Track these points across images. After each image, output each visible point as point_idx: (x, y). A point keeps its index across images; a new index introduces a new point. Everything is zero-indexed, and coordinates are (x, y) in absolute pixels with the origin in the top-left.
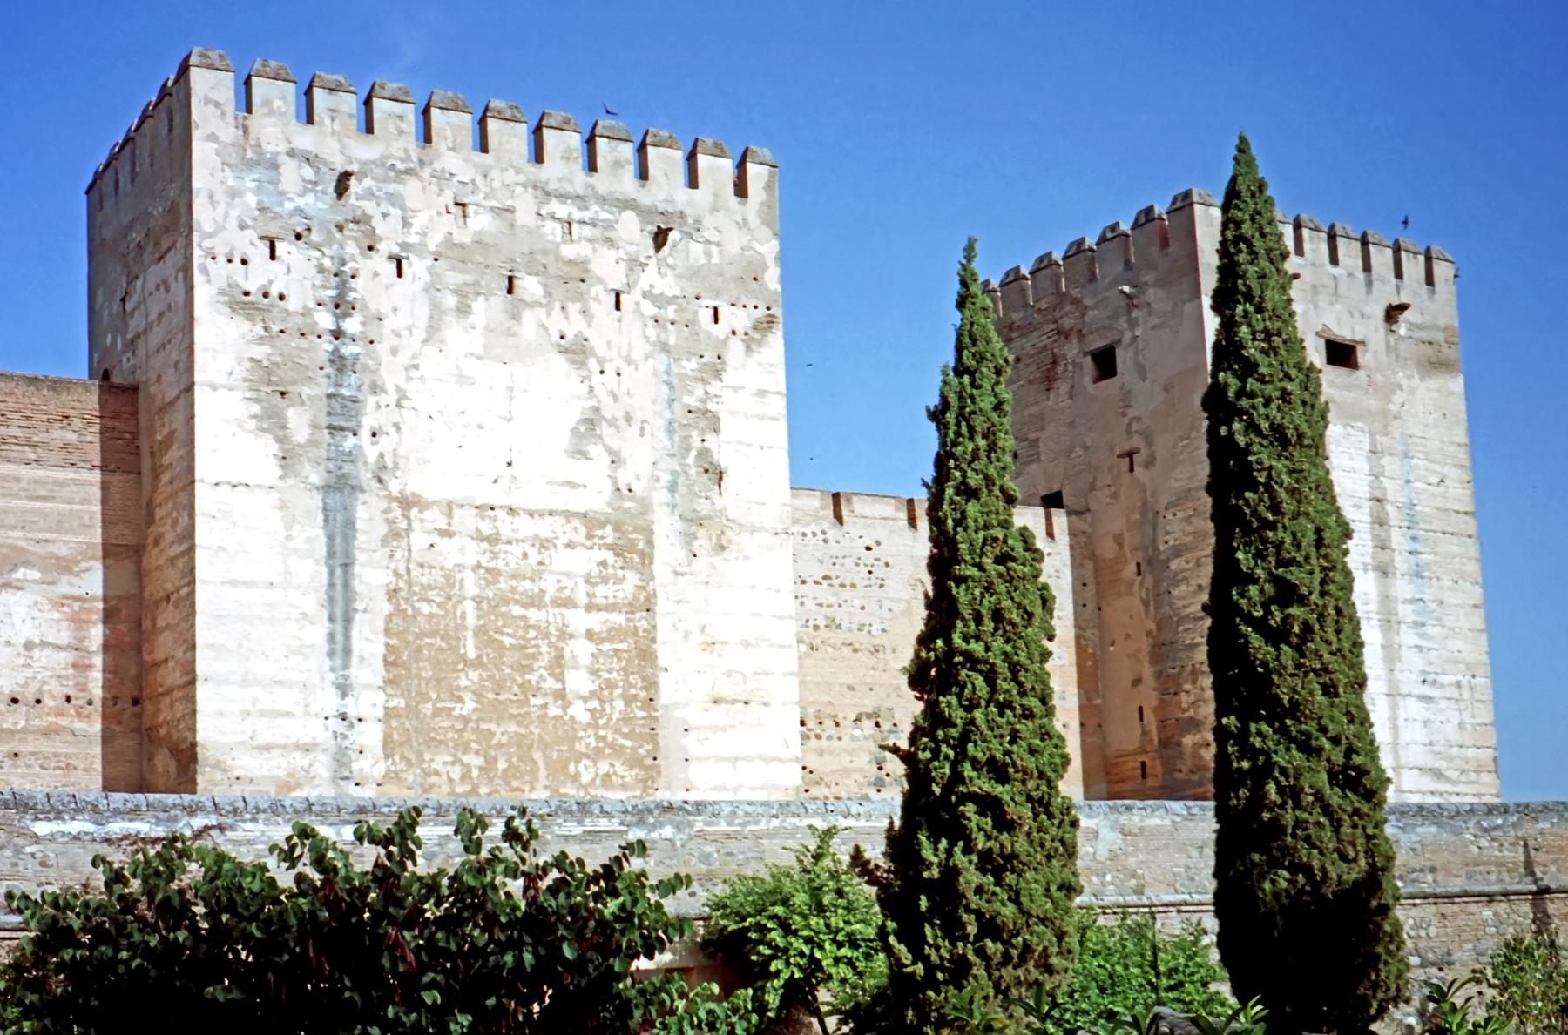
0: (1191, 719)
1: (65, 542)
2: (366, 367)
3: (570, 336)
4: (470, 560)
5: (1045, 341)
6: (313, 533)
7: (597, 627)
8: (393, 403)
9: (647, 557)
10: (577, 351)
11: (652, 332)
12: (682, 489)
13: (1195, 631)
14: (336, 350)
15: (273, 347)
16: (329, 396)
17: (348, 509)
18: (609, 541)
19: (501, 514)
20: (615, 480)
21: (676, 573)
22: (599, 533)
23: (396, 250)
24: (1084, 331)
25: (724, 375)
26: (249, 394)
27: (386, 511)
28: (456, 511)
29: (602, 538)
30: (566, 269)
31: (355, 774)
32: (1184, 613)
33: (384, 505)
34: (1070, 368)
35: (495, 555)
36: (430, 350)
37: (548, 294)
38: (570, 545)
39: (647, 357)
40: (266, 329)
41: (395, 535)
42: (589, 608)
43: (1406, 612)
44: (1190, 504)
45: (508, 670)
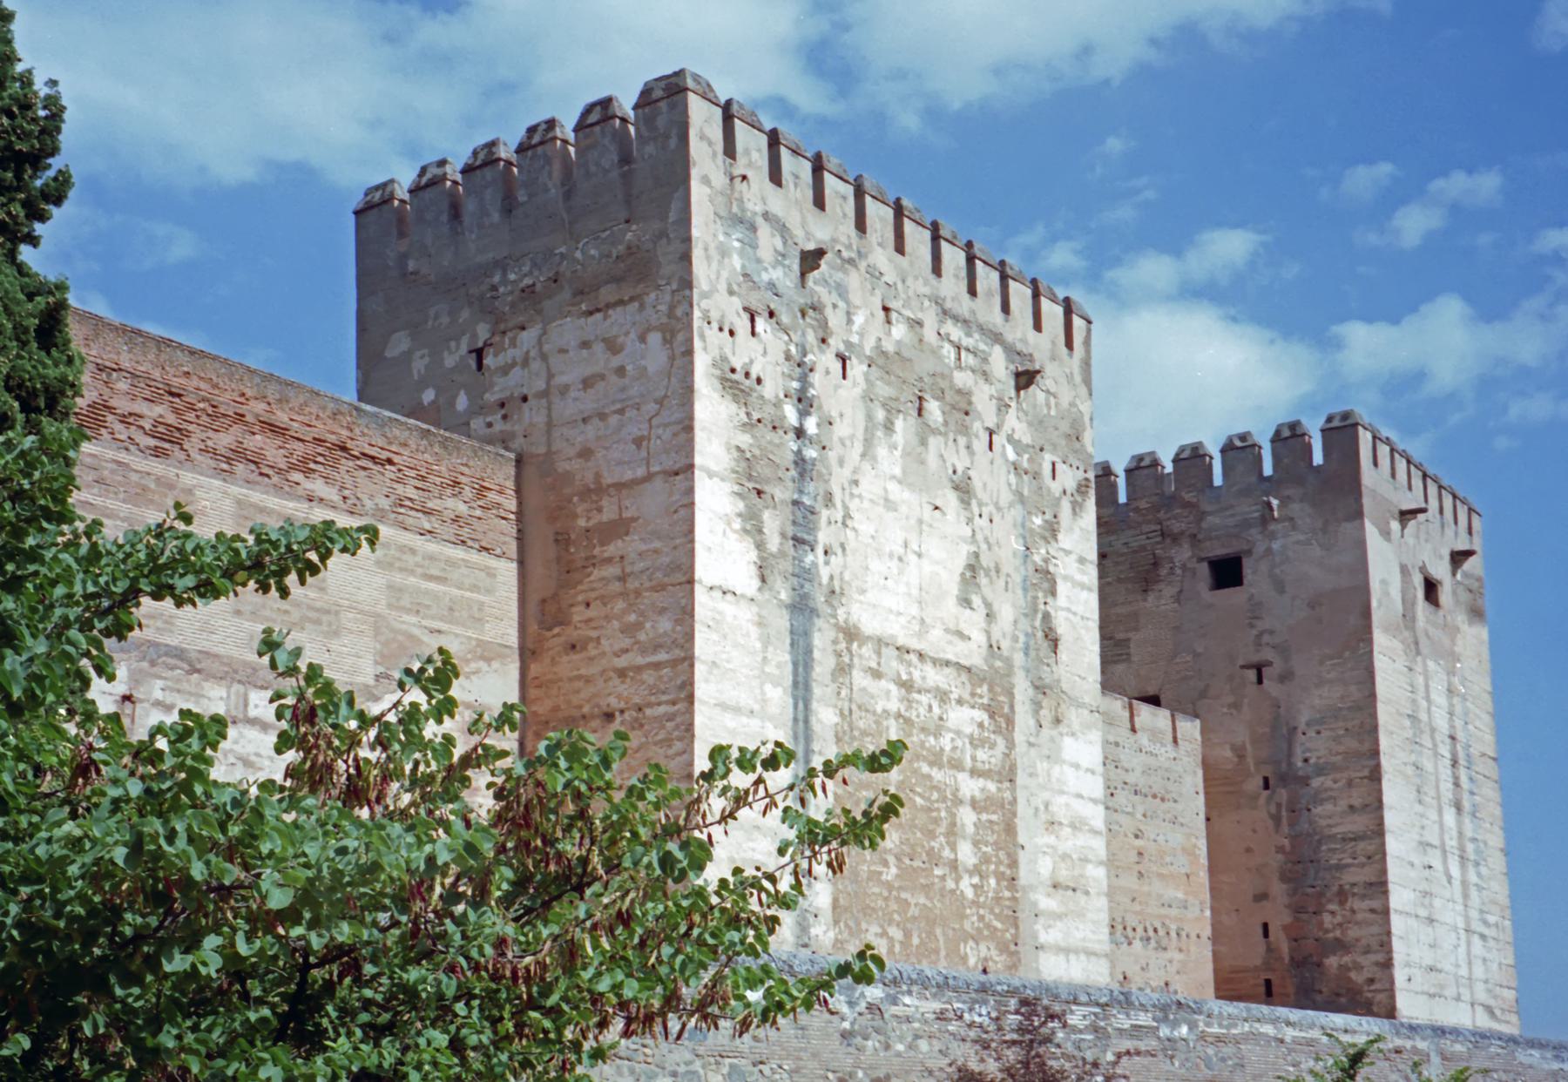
0: (1336, 939)
1: (457, 635)
2: (820, 475)
3: (960, 471)
4: (894, 705)
5: (1142, 541)
6: (781, 656)
7: (978, 794)
8: (840, 520)
9: (1010, 722)
10: (963, 489)
11: (1013, 479)
12: (1033, 653)
13: (1344, 852)
14: (799, 452)
15: (753, 436)
16: (796, 503)
17: (807, 634)
18: (985, 701)
19: (913, 658)
20: (989, 638)
21: (1031, 744)
22: (979, 691)
23: (842, 348)
24: (1200, 536)
25: (1060, 537)
26: (736, 488)
27: (835, 642)
28: (884, 650)
29: (981, 697)
30: (958, 398)
31: (812, 942)
32: (1327, 832)
33: (832, 634)
34: (1179, 571)
35: (910, 703)
36: (866, 466)
37: (946, 423)
38: (960, 702)
39: (1011, 505)
40: (748, 414)
41: (842, 670)
42: (975, 773)
43: (1470, 847)
44: (1341, 724)
45: (919, 835)
